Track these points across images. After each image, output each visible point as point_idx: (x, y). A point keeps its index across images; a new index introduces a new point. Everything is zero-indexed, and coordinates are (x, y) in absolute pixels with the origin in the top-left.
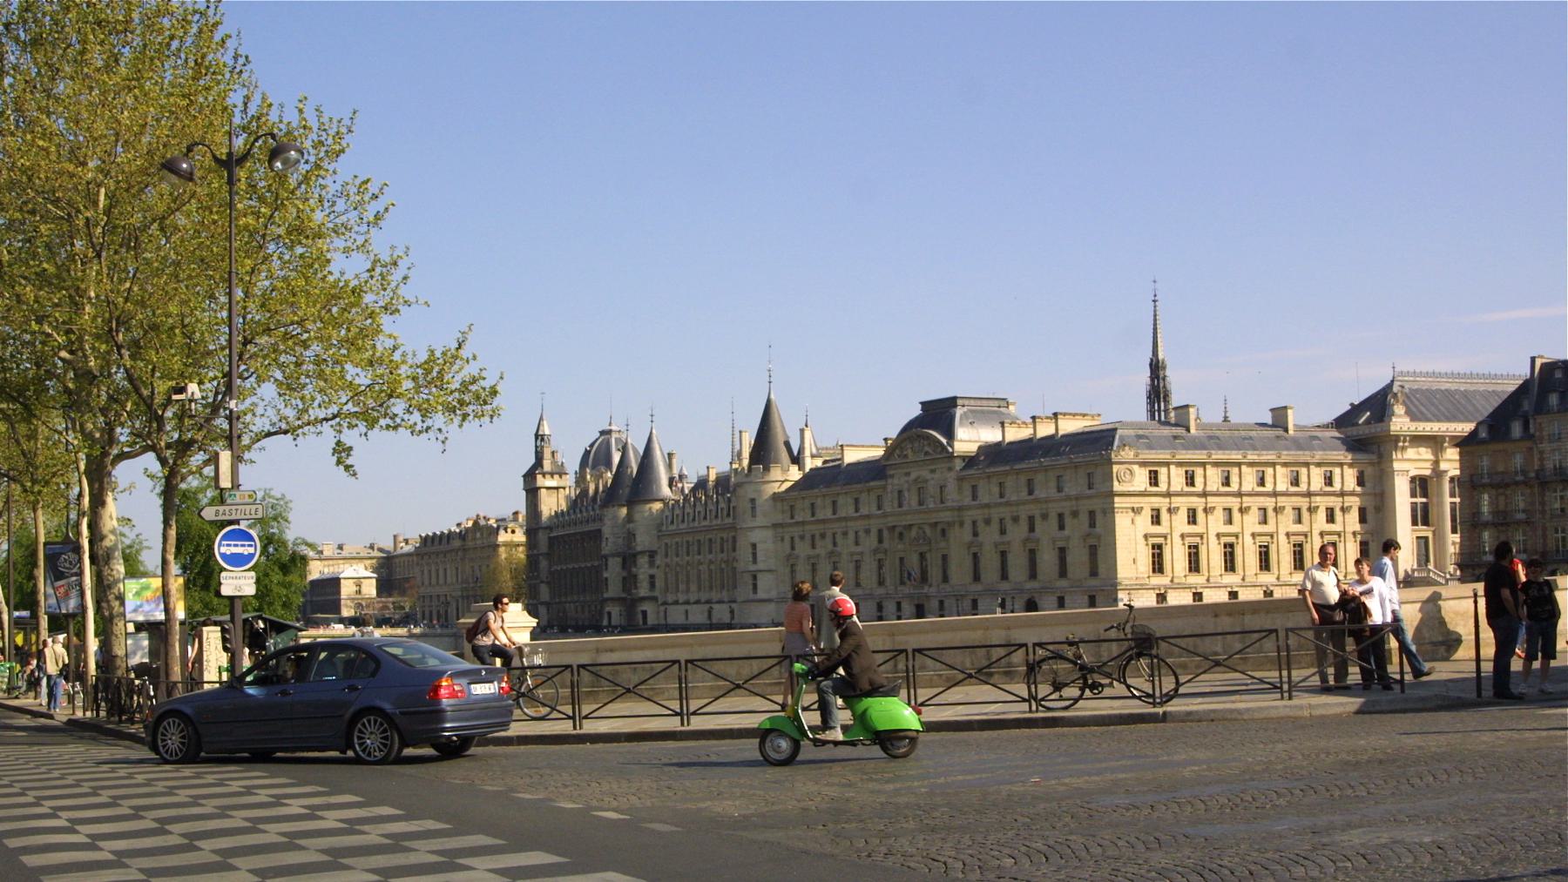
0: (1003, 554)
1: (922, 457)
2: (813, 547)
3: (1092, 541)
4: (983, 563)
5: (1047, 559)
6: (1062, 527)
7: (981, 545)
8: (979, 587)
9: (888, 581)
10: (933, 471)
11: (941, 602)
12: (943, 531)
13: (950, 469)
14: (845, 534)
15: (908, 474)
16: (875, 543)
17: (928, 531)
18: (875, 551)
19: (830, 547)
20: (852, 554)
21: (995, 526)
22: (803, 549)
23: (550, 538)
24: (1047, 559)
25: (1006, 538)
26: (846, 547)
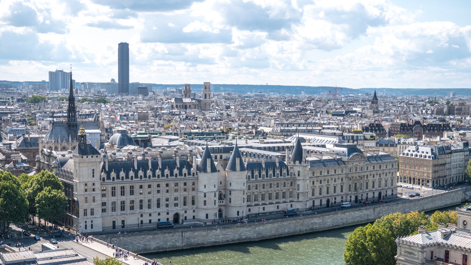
0: (374, 182)
1: (358, 160)
2: (321, 183)
3: (392, 178)
5: (383, 182)
6: (386, 176)
7: (369, 180)
8: (368, 190)
9: (344, 190)
12: (362, 178)
14: (332, 179)
16: (340, 181)
19: (327, 183)
22: (317, 184)
24: (383, 182)
25: (375, 178)
26: (332, 183)
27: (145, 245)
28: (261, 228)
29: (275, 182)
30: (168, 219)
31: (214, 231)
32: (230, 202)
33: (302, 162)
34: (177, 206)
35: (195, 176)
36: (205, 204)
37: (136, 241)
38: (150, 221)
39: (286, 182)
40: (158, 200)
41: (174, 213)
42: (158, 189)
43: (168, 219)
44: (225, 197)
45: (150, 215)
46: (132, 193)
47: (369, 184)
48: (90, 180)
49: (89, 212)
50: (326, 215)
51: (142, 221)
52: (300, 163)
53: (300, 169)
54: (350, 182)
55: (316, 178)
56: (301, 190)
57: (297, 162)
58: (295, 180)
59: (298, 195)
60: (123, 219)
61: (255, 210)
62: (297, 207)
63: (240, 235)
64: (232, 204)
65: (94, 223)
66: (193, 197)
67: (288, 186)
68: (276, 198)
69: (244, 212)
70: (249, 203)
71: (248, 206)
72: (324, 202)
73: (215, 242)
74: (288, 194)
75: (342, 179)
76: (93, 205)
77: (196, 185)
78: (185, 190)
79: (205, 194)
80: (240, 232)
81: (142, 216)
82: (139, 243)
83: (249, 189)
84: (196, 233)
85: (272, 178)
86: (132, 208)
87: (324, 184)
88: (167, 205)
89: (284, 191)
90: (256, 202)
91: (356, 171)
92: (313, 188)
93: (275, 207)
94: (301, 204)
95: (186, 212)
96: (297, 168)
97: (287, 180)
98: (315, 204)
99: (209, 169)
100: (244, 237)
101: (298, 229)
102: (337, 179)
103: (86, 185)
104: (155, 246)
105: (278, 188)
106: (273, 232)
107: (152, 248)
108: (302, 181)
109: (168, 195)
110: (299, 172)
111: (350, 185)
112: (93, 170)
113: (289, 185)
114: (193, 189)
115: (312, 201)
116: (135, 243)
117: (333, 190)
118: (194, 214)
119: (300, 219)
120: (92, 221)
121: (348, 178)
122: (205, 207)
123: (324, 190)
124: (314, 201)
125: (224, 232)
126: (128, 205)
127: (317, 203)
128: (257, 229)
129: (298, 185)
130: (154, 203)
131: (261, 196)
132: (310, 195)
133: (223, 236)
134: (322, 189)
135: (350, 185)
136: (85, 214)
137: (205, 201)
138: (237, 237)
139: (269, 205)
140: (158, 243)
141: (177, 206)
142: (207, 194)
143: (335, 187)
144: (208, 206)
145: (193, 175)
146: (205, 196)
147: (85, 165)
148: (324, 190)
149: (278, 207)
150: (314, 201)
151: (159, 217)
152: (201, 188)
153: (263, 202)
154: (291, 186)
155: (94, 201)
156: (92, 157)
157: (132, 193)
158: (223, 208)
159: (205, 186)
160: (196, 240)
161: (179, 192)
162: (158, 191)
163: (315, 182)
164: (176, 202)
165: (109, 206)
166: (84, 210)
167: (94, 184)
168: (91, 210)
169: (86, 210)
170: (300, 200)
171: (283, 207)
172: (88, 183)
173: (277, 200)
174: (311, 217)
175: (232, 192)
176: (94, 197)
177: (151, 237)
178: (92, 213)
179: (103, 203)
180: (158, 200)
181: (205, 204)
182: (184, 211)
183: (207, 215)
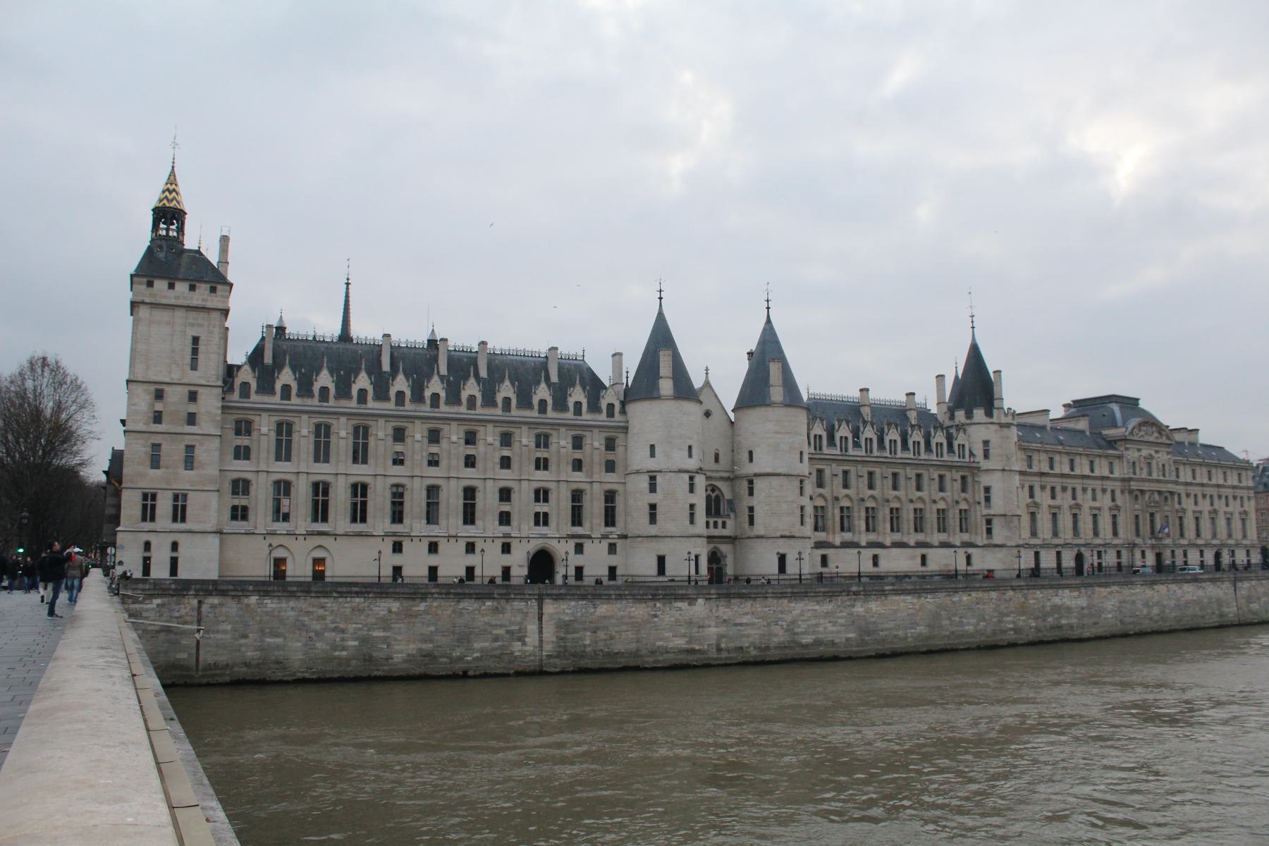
1: (1152, 439)
2: (1053, 497)
4: (1070, 524)
7: (1184, 511)
9: (1121, 531)
10: (1157, 452)
11: (1173, 552)
12: (1166, 498)
13: (1168, 453)
14: (1084, 490)
15: (1139, 450)
17: (1156, 497)
18: (1110, 509)
20: (1091, 508)
21: (1192, 500)
22: (1043, 498)
23: (223, 408)
27: (364, 640)
28: (875, 606)
29: (908, 469)
30: (506, 571)
31: (683, 605)
32: (751, 522)
33: (995, 412)
34: (546, 523)
35: (617, 416)
36: (653, 519)
37: (323, 618)
38: (433, 570)
39: (948, 475)
40: (470, 493)
41: (533, 546)
42: (470, 450)
43: (506, 571)
44: (733, 510)
45: (433, 548)
46: (360, 454)
47: (1186, 522)
48: (175, 377)
49: (164, 506)
50: (1100, 585)
51: (397, 570)
52: (989, 414)
53: (990, 433)
54: (1137, 507)
55: (1037, 479)
56: (998, 505)
57: (979, 414)
58: (975, 469)
59: (989, 522)
60: (319, 554)
61: (846, 563)
62: (987, 566)
63: (790, 630)
64: (759, 529)
65: (182, 553)
66: (610, 496)
67: (953, 489)
68: (916, 530)
69: (805, 563)
70: (821, 536)
71: (819, 545)
72: (1068, 561)
73: (691, 651)
74: (953, 519)
75: (1113, 492)
76: (184, 479)
77: (620, 449)
78: (578, 465)
79: (653, 478)
80: (789, 618)
81: (397, 548)
82: (335, 630)
83: (820, 484)
84: (603, 609)
85: (899, 454)
86: (359, 513)
87: (1064, 500)
88: (505, 518)
89: (942, 505)
90: (848, 536)
91: (1150, 474)
92: (1032, 510)
93: (913, 558)
94: (1000, 554)
95: (579, 549)
96: (979, 431)
97: (950, 467)
98: (1043, 565)
99: (666, 386)
100: (807, 639)
101: (1009, 622)
102: (1099, 494)
103: (159, 395)
104: (412, 648)
105: (919, 494)
106: (922, 629)
107: (398, 658)
108: (999, 474)
109: (506, 477)
110: (986, 443)
111: (1137, 517)
112: (196, 340)
113: (958, 485)
114: (610, 467)
115: (1032, 554)
116: (317, 626)
117: (1091, 526)
118: (613, 560)
119: (1013, 588)
120: (175, 546)
121: (1131, 492)
122: (653, 530)
123: (1065, 521)
124: (1037, 554)
125: (724, 611)
126: (340, 499)
127: (1048, 561)
128: (859, 609)
129: (987, 489)
130: (452, 500)
131: (863, 514)
132: (1026, 533)
133: (722, 630)
134: (1060, 517)
135: (1137, 517)
136: (148, 513)
137: (653, 507)
138: (779, 636)
139: (895, 551)
140: (426, 639)
141: (546, 523)
142: (659, 479)
143: (1095, 516)
144: (665, 524)
145: (610, 412)
146: (653, 488)
147: (161, 315)
148: (1065, 521)
149: (924, 558)
150: (1037, 554)
151: (472, 560)
152: (638, 458)
153: (872, 537)
154: (964, 490)
155: (189, 462)
156: (192, 288)
157: (360, 454)
158: (725, 548)
159: (652, 447)
160: (601, 635)
161: (552, 466)
162: (470, 462)
163: (1037, 490)
164: (542, 508)
165: (261, 497)
166: (145, 496)
167: (193, 397)
168: (176, 498)
169: (154, 497)
170: (998, 537)
171: (940, 560)
172: (167, 389)
173: (920, 537)
174: (1051, 587)
175: (759, 484)
176: (190, 448)
177: (395, 606)
178: (179, 513)
179: (235, 483)
180: (470, 493)
181: (653, 519)
182: (571, 545)
183: (661, 560)
